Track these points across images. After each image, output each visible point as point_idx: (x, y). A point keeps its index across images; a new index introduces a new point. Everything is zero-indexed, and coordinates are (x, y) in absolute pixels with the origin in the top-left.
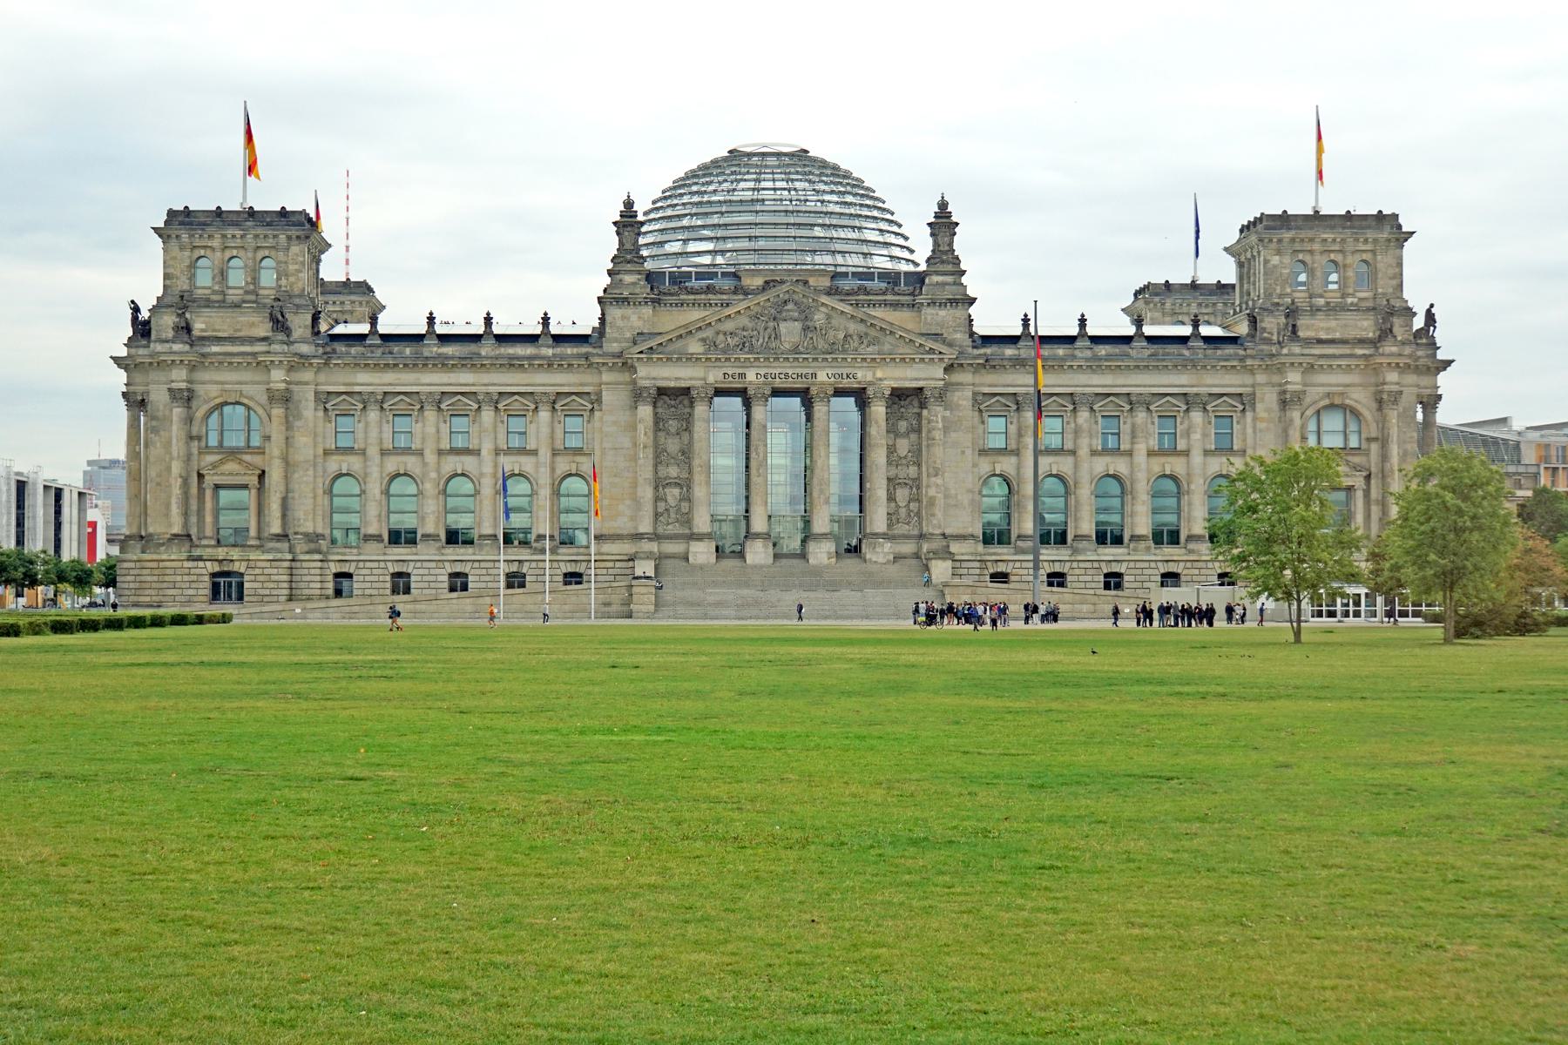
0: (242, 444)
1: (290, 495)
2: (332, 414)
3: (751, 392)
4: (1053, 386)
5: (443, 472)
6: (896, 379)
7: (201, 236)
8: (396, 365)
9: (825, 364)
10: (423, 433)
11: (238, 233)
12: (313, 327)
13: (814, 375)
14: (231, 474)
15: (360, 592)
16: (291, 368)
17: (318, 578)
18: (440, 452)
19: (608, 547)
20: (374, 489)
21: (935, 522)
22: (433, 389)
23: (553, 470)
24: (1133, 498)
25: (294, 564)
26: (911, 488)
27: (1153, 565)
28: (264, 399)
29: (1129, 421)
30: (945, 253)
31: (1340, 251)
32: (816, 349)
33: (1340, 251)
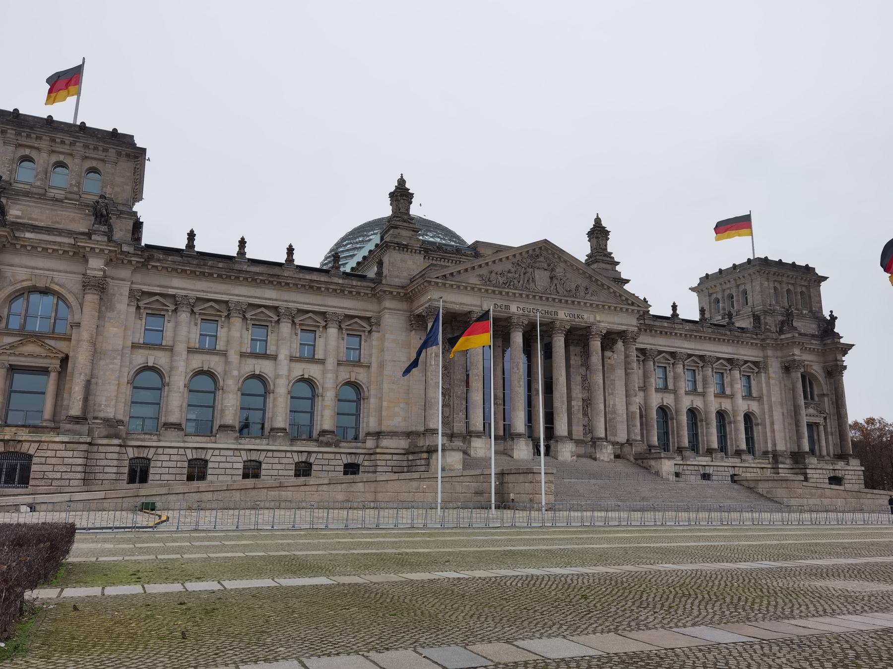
0: (47, 329)
1: (93, 380)
2: (144, 313)
4: (665, 346)
5: (243, 372)
7: (28, 136)
8: (211, 275)
10: (228, 336)
11: (68, 139)
12: (133, 234)
13: (556, 313)
14: (30, 355)
15: (157, 477)
16: (109, 262)
17: (115, 463)
18: (243, 355)
19: (386, 442)
20: (179, 381)
24: (707, 424)
27: (726, 469)
28: (77, 287)
29: (701, 373)
31: (792, 284)
32: (558, 293)
33: (792, 284)
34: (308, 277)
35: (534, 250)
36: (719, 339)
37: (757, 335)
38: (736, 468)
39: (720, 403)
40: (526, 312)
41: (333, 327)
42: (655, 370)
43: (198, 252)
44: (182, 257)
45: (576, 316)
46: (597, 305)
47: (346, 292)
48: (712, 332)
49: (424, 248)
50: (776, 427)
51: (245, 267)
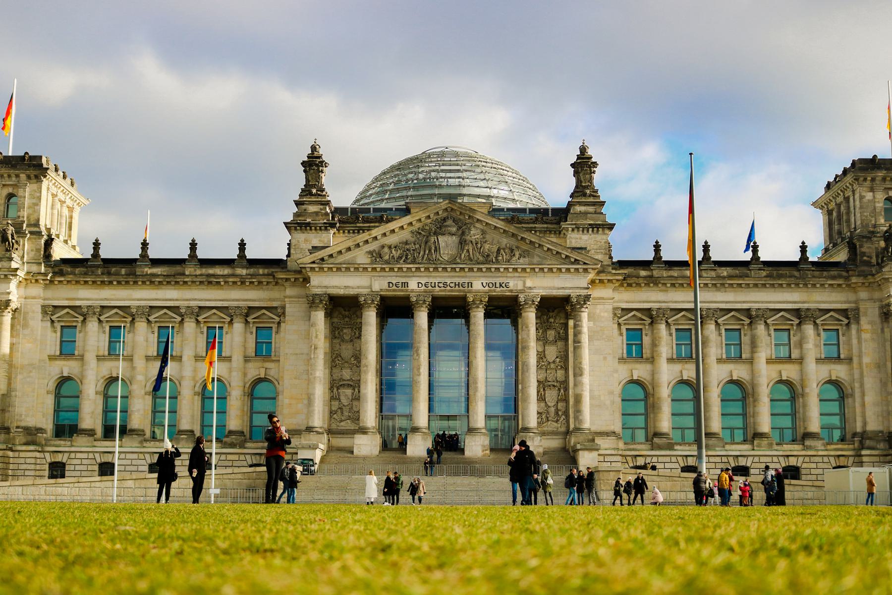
1: (13, 394)
3: (414, 299)
4: (683, 302)
6: (544, 288)
8: (111, 283)
9: (479, 274)
12: (45, 251)
17: (33, 467)
21: (580, 418)
22: (143, 303)
23: (245, 375)
24: (755, 400)
25: (11, 454)
26: (559, 390)
29: (749, 333)
30: (587, 187)
32: (471, 260)
34: (211, 271)
35: (438, 213)
36: (773, 284)
37: (847, 272)
38: (790, 458)
39: (780, 372)
40: (430, 288)
41: (237, 322)
42: (671, 335)
43: (103, 260)
44: (87, 267)
45: (498, 285)
46: (524, 270)
47: (247, 284)
48: (766, 277)
49: (329, 224)
50: (867, 399)
51: (146, 270)
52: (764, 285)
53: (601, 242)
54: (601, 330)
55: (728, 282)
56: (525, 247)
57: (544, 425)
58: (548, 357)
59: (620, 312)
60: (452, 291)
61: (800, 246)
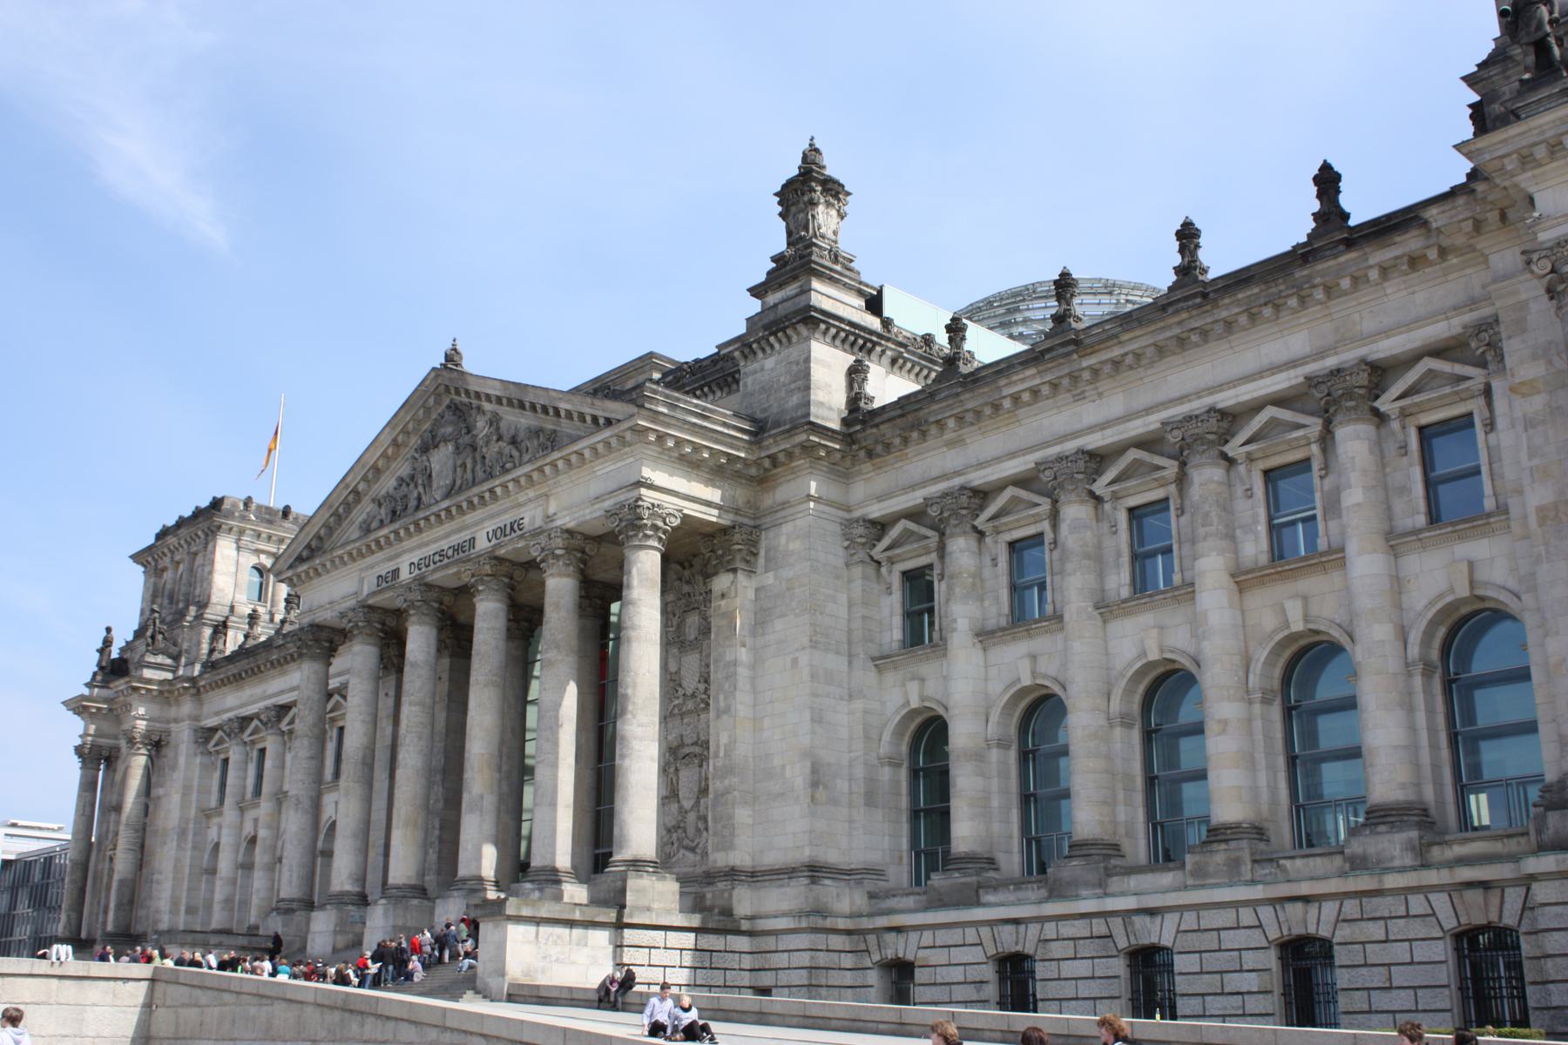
1: (156, 877)
4: (998, 460)
12: (211, 643)
26: (701, 766)
27: (1247, 916)
38: (1289, 907)
40: (424, 569)
42: (994, 561)
45: (508, 531)
52: (1182, 342)
53: (798, 363)
54: (788, 589)
55: (1085, 363)
56: (549, 424)
57: (674, 859)
58: (685, 684)
59: (861, 530)
60: (447, 566)
61: (1316, 180)
